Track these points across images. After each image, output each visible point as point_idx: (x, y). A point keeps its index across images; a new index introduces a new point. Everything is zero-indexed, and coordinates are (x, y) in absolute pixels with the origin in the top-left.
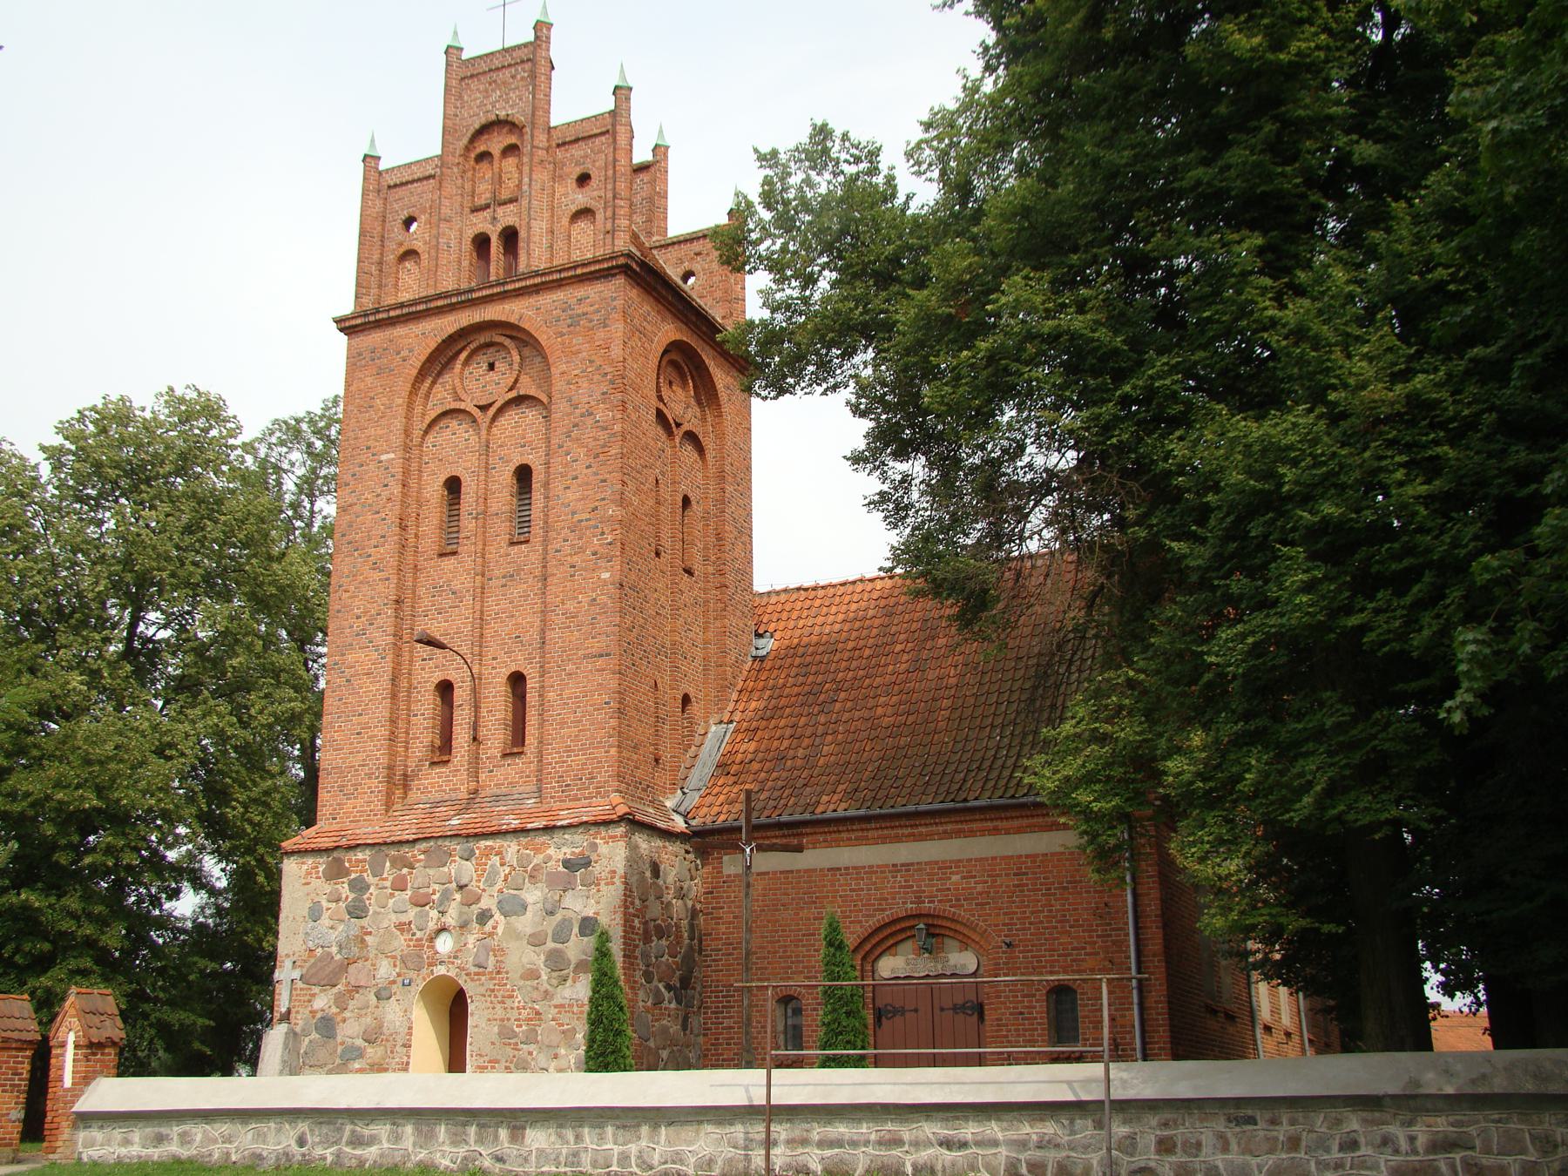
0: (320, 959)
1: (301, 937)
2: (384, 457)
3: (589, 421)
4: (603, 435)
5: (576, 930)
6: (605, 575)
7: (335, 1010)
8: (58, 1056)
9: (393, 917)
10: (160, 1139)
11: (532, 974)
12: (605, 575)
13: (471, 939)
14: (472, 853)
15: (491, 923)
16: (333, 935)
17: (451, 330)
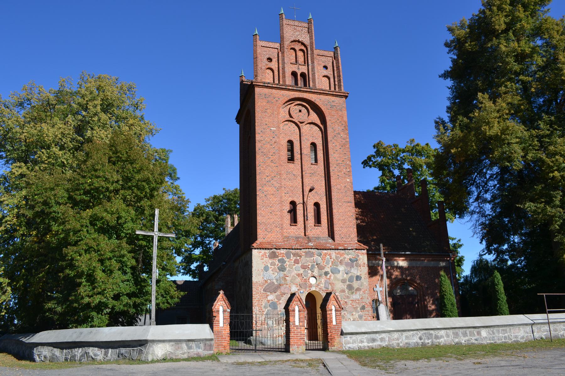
0: (270, 284)
1: (262, 276)
2: (272, 129)
3: (339, 136)
4: (344, 141)
5: (355, 279)
6: (348, 180)
7: (276, 300)
8: (330, 312)
9: (296, 272)
10: (374, 340)
11: (343, 291)
12: (348, 180)
13: (323, 281)
14: (321, 254)
15: (329, 275)
16: (274, 276)
17: (297, 96)
